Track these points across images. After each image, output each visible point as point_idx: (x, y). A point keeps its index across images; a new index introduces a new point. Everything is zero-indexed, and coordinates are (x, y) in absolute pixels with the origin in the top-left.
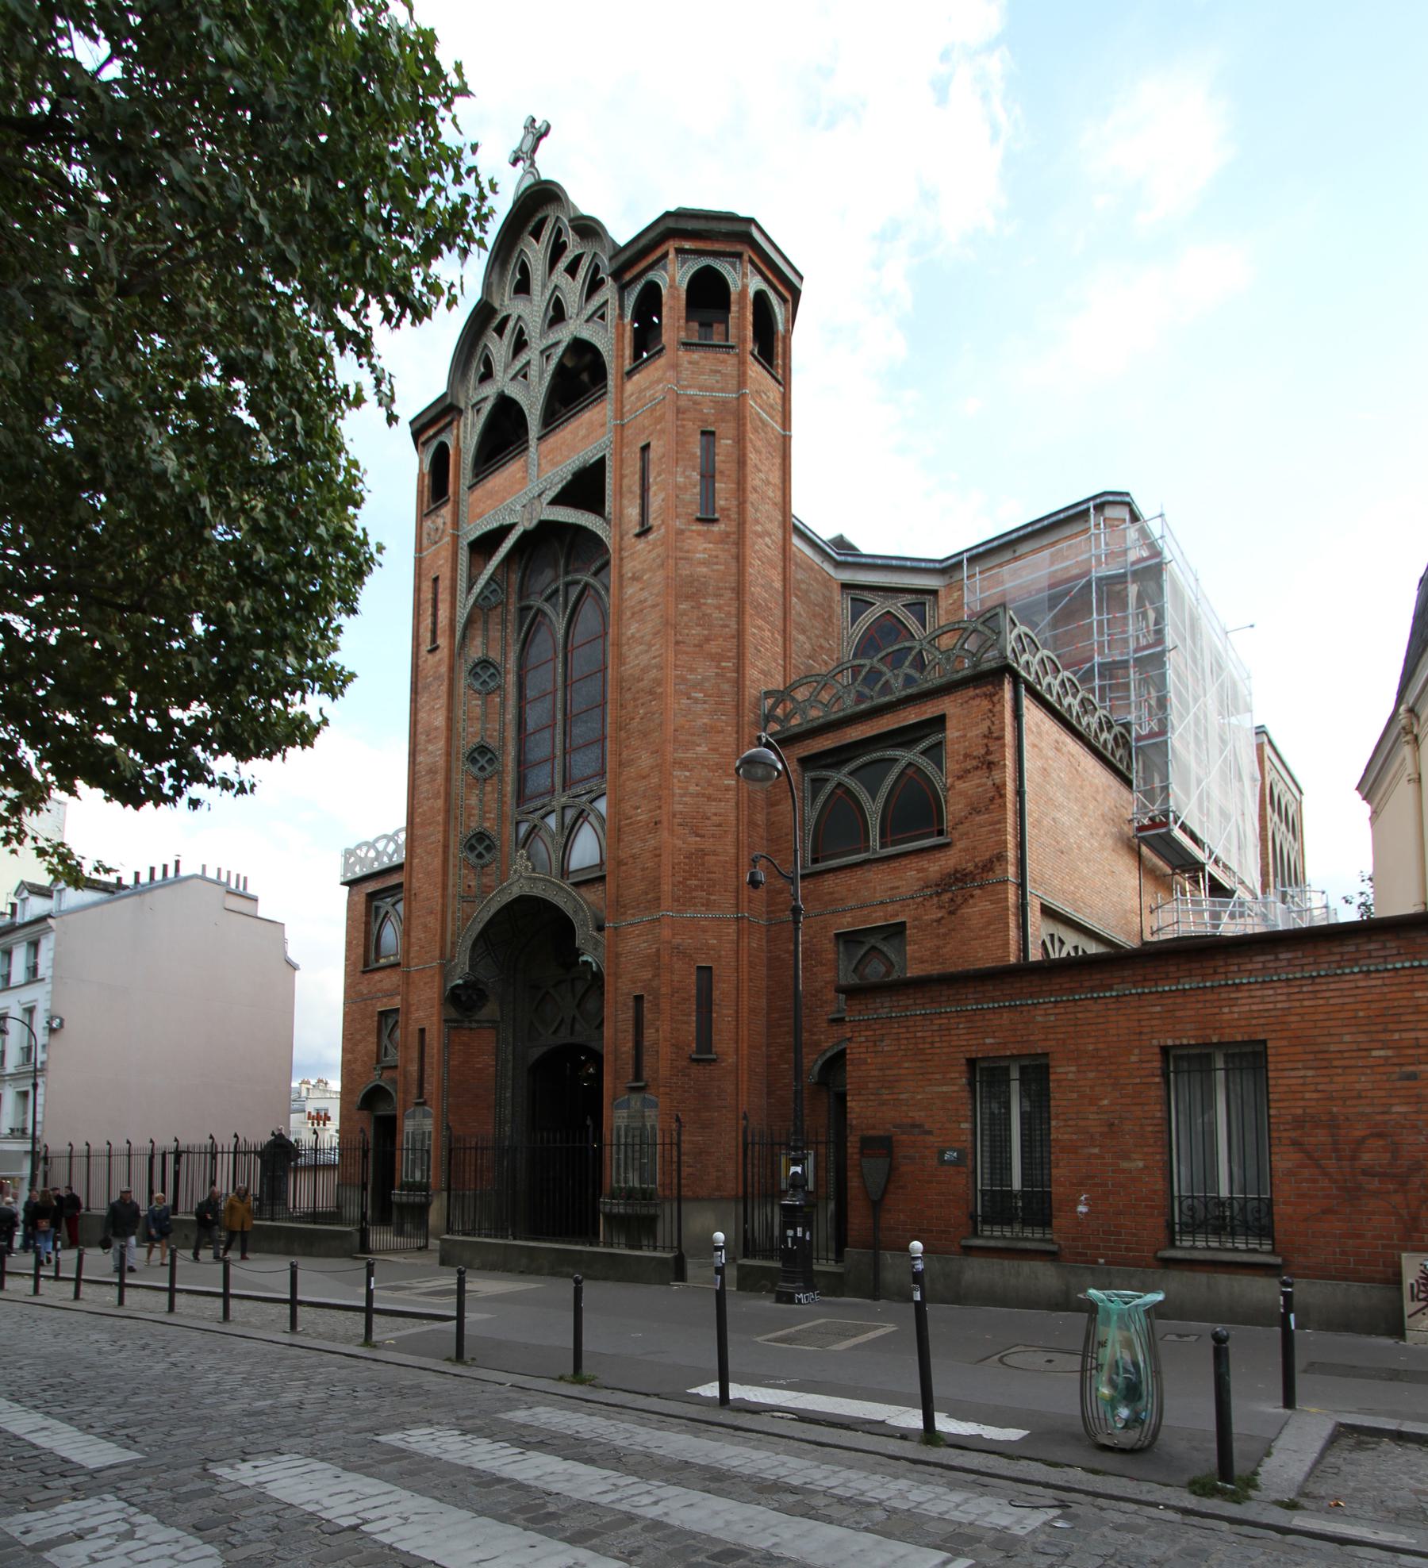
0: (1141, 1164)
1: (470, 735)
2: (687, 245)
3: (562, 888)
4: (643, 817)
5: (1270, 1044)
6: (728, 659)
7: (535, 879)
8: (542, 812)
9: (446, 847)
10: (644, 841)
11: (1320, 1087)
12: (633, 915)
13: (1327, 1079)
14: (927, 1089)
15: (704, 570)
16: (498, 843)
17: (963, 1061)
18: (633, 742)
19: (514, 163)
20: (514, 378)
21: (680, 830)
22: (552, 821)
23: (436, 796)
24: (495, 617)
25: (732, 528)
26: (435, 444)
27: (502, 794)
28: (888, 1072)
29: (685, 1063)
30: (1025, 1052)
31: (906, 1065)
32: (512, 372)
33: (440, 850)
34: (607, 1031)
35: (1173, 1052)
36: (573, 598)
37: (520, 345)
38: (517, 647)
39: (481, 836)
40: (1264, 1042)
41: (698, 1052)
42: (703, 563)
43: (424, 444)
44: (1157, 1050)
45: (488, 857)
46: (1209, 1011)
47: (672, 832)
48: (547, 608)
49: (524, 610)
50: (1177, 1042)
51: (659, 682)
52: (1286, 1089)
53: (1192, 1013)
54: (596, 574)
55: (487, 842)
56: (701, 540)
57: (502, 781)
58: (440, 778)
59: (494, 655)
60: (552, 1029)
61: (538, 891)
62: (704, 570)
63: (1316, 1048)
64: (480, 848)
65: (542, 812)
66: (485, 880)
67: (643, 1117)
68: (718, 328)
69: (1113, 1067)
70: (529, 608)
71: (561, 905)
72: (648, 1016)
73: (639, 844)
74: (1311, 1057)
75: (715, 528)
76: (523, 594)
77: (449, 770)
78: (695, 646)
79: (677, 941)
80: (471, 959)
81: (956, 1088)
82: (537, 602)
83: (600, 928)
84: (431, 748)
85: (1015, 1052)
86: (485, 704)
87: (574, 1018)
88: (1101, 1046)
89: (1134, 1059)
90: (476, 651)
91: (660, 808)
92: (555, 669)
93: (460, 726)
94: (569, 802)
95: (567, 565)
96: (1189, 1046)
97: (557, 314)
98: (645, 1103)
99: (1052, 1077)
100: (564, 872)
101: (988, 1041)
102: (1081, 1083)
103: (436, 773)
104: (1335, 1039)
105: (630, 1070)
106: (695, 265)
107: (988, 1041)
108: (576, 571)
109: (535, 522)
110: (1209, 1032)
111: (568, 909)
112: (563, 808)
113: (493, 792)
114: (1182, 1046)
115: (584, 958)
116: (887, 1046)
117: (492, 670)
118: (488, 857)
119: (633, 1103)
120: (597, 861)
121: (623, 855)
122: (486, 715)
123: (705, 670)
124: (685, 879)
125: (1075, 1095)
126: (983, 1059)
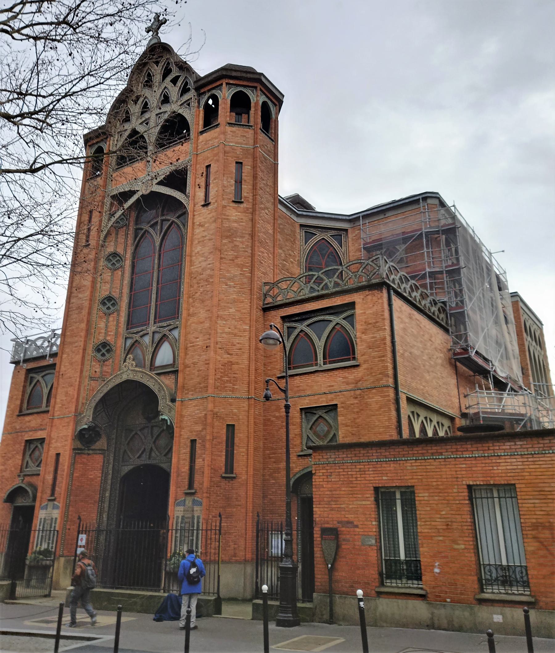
0: (463, 547)
1: (104, 291)
2: (231, 82)
3: (152, 377)
4: (200, 342)
5: (517, 486)
6: (247, 267)
7: (137, 371)
8: (141, 333)
9: (84, 350)
10: (200, 355)
11: (543, 509)
12: (192, 395)
13: (545, 505)
14: (355, 503)
15: (235, 225)
16: (114, 348)
17: (372, 488)
18: (197, 304)
19: (148, 32)
20: (141, 124)
21: (219, 351)
22: (147, 340)
23: (81, 321)
24: (122, 233)
25: (250, 206)
26: (96, 146)
27: (118, 322)
28: (334, 492)
29: (218, 479)
30: (403, 485)
31: (343, 489)
32: (140, 121)
33: (81, 351)
34: (174, 460)
35: (474, 487)
36: (165, 228)
37: (145, 108)
38: (133, 248)
39: (104, 345)
40: (514, 484)
41: (226, 473)
42: (236, 221)
43: (90, 146)
44: (466, 487)
45: (107, 355)
46: (487, 468)
47: (215, 352)
48: (151, 230)
49: (137, 231)
50: (475, 483)
51: (211, 276)
52: (527, 509)
53: (480, 468)
54: (178, 217)
55: (108, 347)
56: (234, 210)
57: (119, 315)
58: (85, 312)
59: (120, 250)
60: (138, 455)
61: (138, 378)
62: (235, 225)
63: (539, 489)
64: (104, 351)
65: (141, 333)
66: (105, 368)
67: (193, 511)
68: (245, 116)
69: (446, 494)
70: (142, 229)
71: (151, 387)
72: (198, 451)
73: (197, 357)
74: (537, 493)
75: (242, 206)
76: (137, 221)
77: (90, 308)
78: (230, 260)
79: (216, 410)
80: (94, 413)
81: (369, 503)
82: (146, 227)
83: (173, 400)
84: (80, 295)
85: (397, 484)
86: (112, 275)
87: (151, 449)
88: (439, 483)
89: (455, 490)
90: (110, 249)
91: (209, 339)
92: (154, 260)
93: (98, 285)
94: (158, 330)
95: (162, 211)
96: (480, 485)
97: (166, 100)
98: (195, 502)
99: (417, 498)
100: (152, 367)
101: (384, 478)
102: (431, 502)
103: (82, 309)
104: (547, 485)
105: (187, 483)
106: (234, 90)
107: (384, 478)
108: (167, 215)
109: (148, 192)
110: (489, 479)
111: (155, 389)
112: (154, 333)
113: (113, 321)
114: (477, 485)
115: (164, 417)
116: (334, 478)
117: (118, 258)
118: (107, 355)
119: (187, 502)
120: (171, 362)
121: (187, 362)
122: (112, 280)
123: (235, 271)
124: (222, 377)
125: (428, 509)
126: (382, 487)
